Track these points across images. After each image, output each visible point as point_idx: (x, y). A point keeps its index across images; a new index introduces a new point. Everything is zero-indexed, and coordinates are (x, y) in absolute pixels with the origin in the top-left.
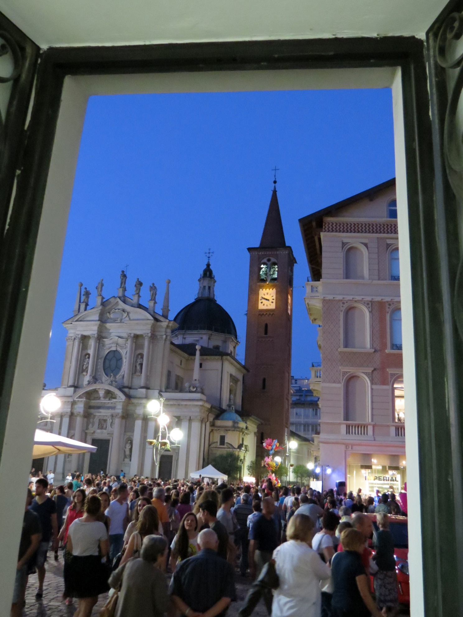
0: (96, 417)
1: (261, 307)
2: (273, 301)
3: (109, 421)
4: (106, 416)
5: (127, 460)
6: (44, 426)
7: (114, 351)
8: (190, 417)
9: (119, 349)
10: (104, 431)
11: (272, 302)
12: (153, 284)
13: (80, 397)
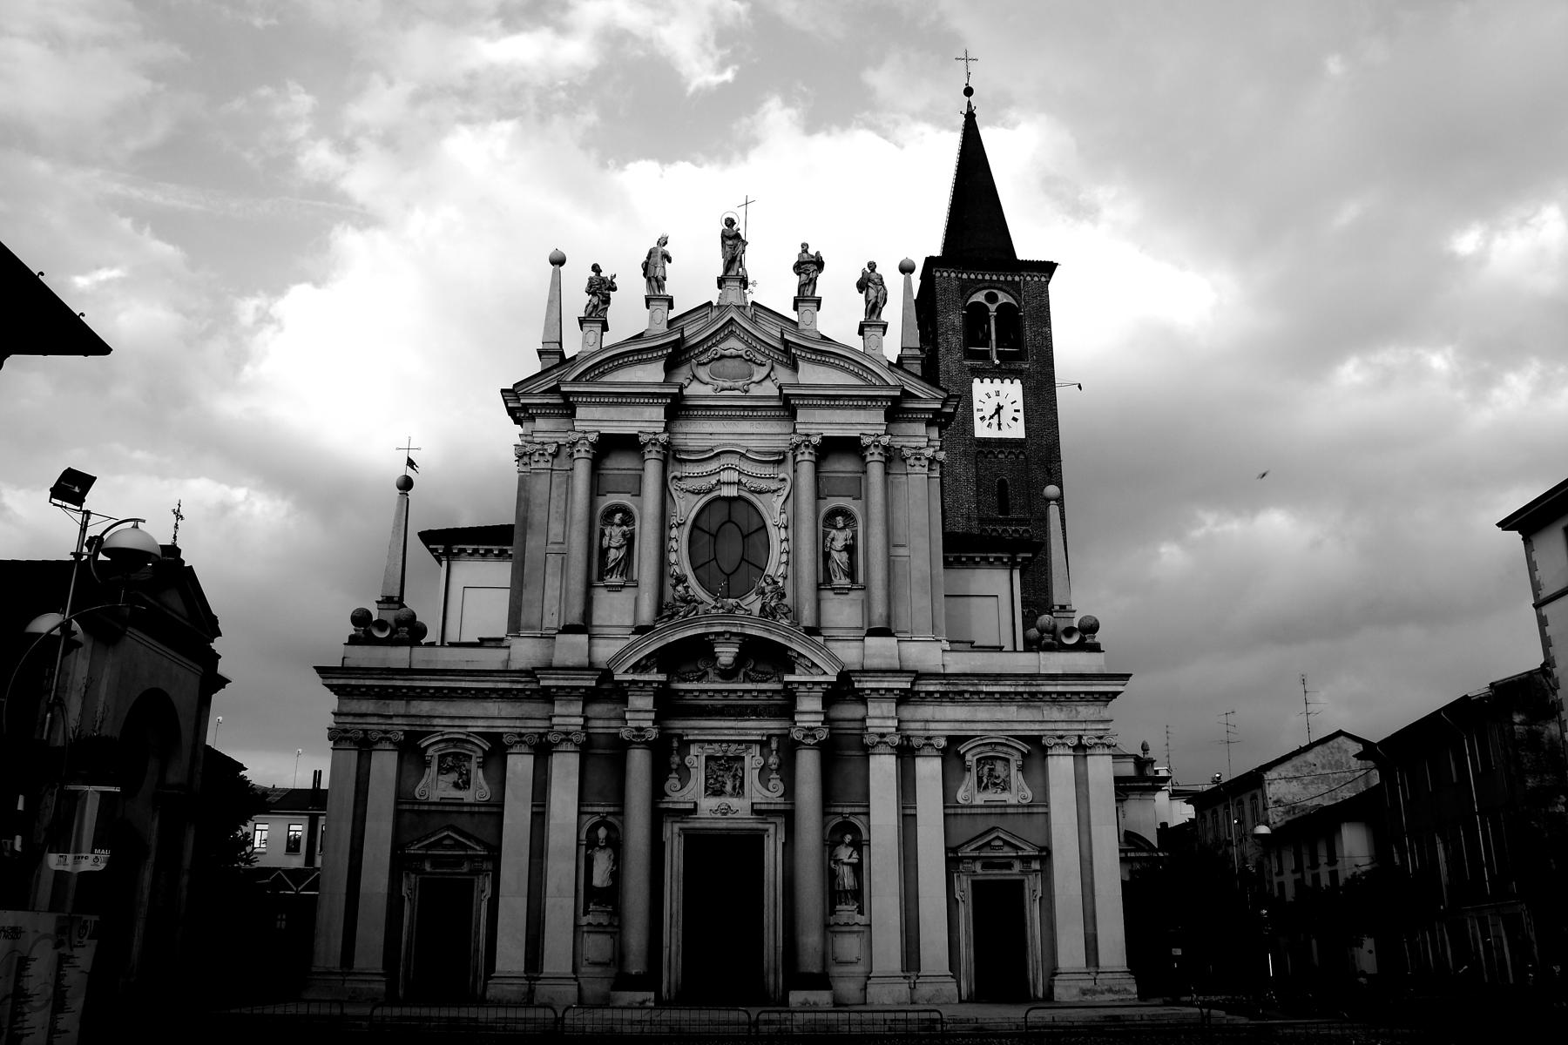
0: (694, 750)
1: (982, 431)
2: (1016, 415)
3: (753, 761)
4: (740, 742)
5: (846, 912)
6: (456, 785)
7: (730, 500)
8: (1080, 737)
9: (744, 494)
10: (734, 802)
11: (1015, 419)
12: (872, 266)
13: (637, 667)
